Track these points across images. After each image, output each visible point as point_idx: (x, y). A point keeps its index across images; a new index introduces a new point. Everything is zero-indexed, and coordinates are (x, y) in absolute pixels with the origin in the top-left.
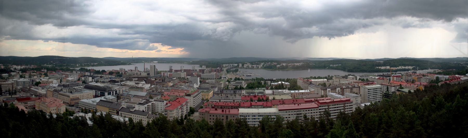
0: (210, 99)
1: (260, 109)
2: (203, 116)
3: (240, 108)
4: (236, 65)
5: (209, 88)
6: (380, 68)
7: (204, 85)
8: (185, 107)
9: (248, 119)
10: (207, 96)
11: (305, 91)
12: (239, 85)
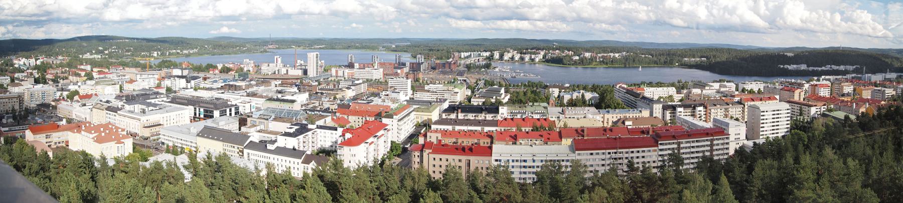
6: (786, 66)
12: (494, 97)
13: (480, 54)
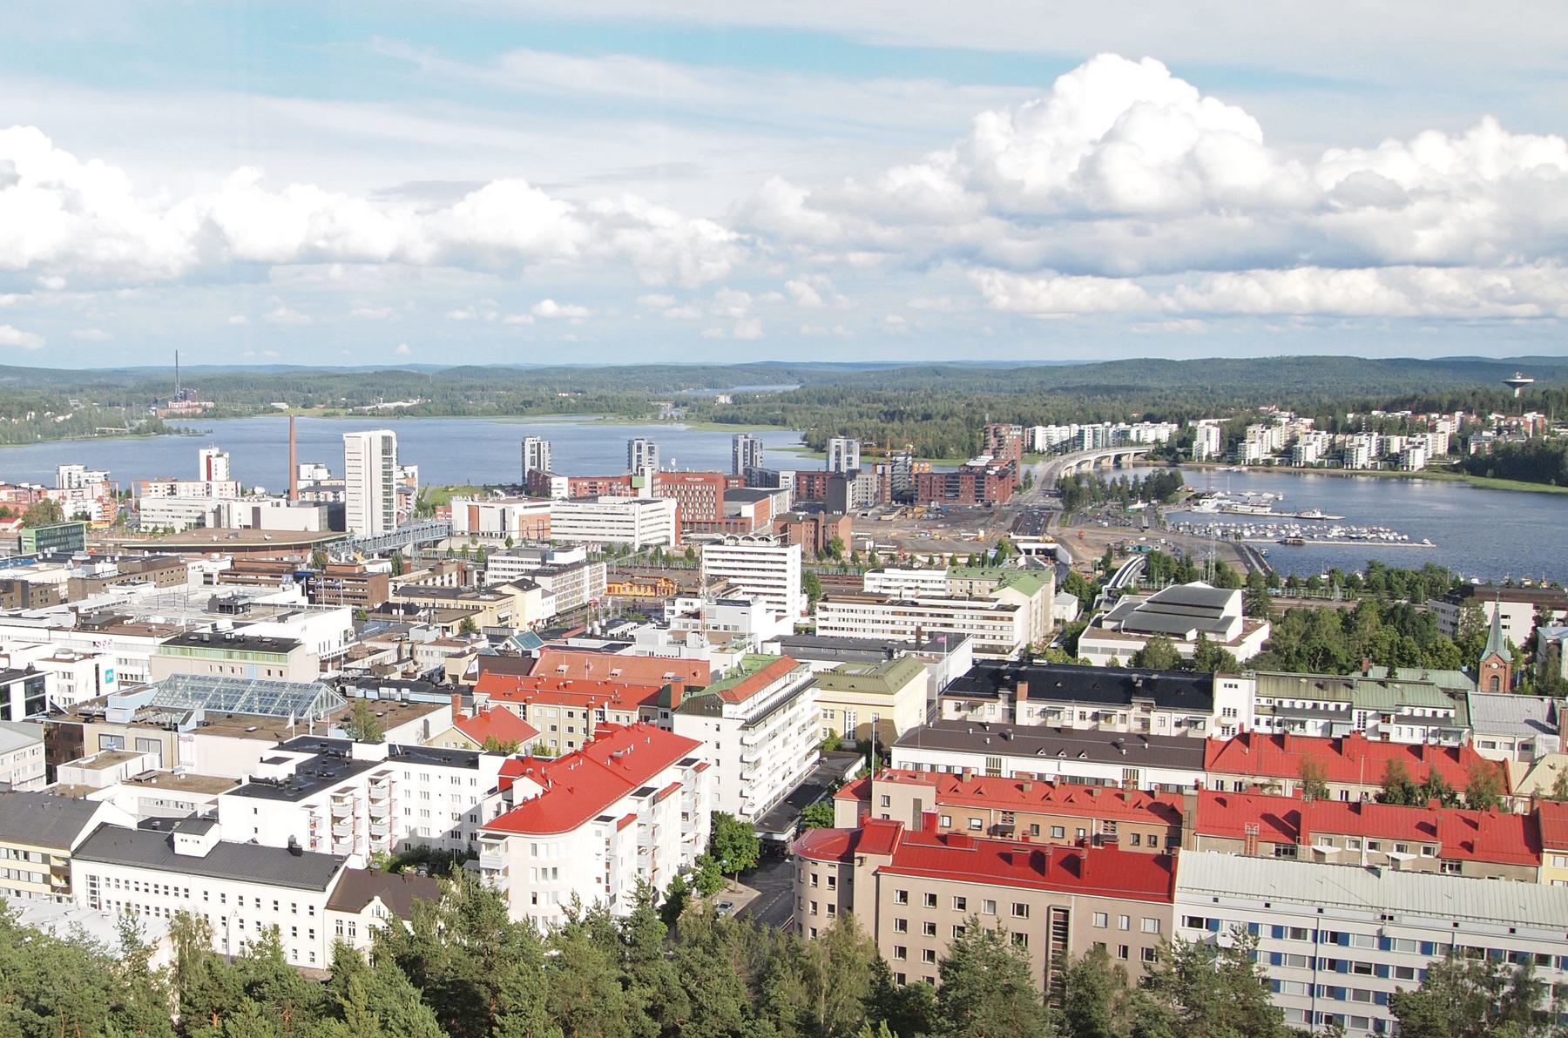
7: (837, 619)
12: (1192, 635)
13: (1125, 433)
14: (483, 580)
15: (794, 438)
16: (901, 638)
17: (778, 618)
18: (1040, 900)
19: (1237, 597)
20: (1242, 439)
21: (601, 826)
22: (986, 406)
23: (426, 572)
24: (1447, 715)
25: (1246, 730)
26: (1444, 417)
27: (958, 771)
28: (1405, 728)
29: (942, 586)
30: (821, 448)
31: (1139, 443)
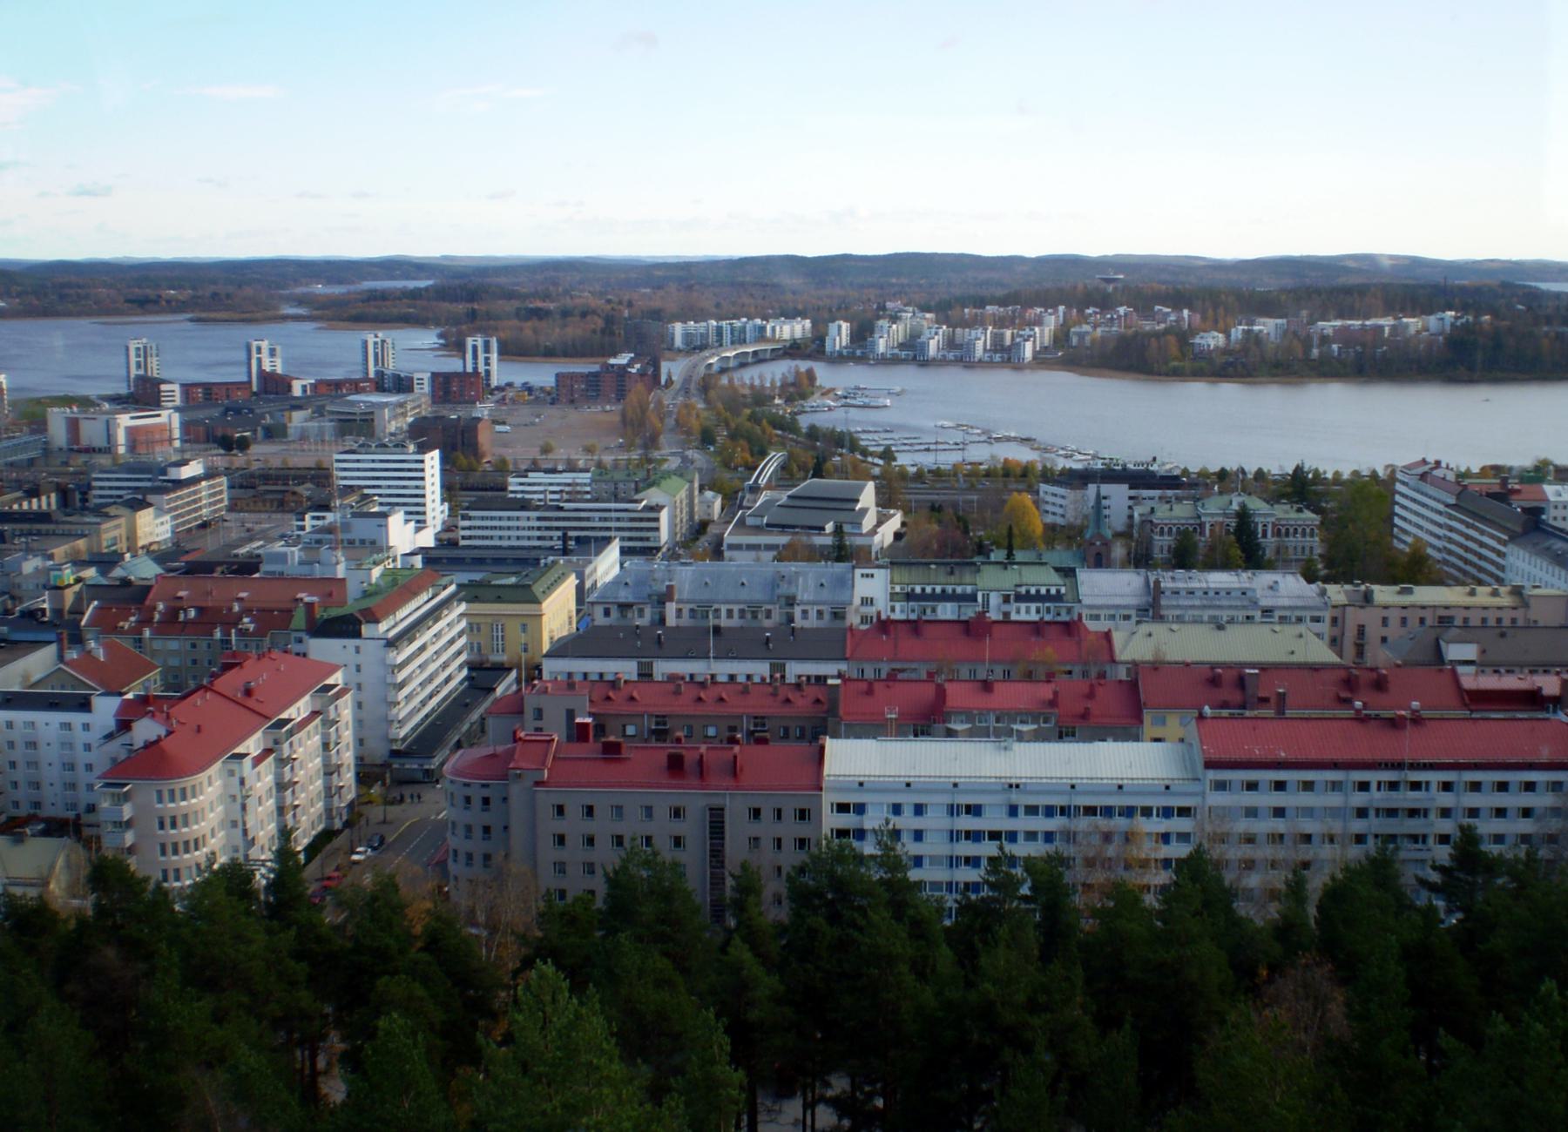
0: (549, 655)
1: (1020, 748)
2: (487, 818)
3: (835, 735)
4: (796, 329)
5: (534, 554)
8: (306, 747)
9: (906, 838)
10: (524, 627)
11: (1472, 593)
12: (829, 527)
13: (763, 329)
14: (87, 500)
15: (428, 338)
16: (548, 543)
17: (418, 530)
18: (696, 801)
19: (870, 487)
20: (872, 332)
21: (234, 766)
22: (625, 304)
23: (19, 494)
24: (1058, 591)
25: (883, 617)
26: (1049, 311)
27: (610, 677)
28: (1023, 606)
29: (588, 489)
30: (458, 347)
31: (773, 340)
